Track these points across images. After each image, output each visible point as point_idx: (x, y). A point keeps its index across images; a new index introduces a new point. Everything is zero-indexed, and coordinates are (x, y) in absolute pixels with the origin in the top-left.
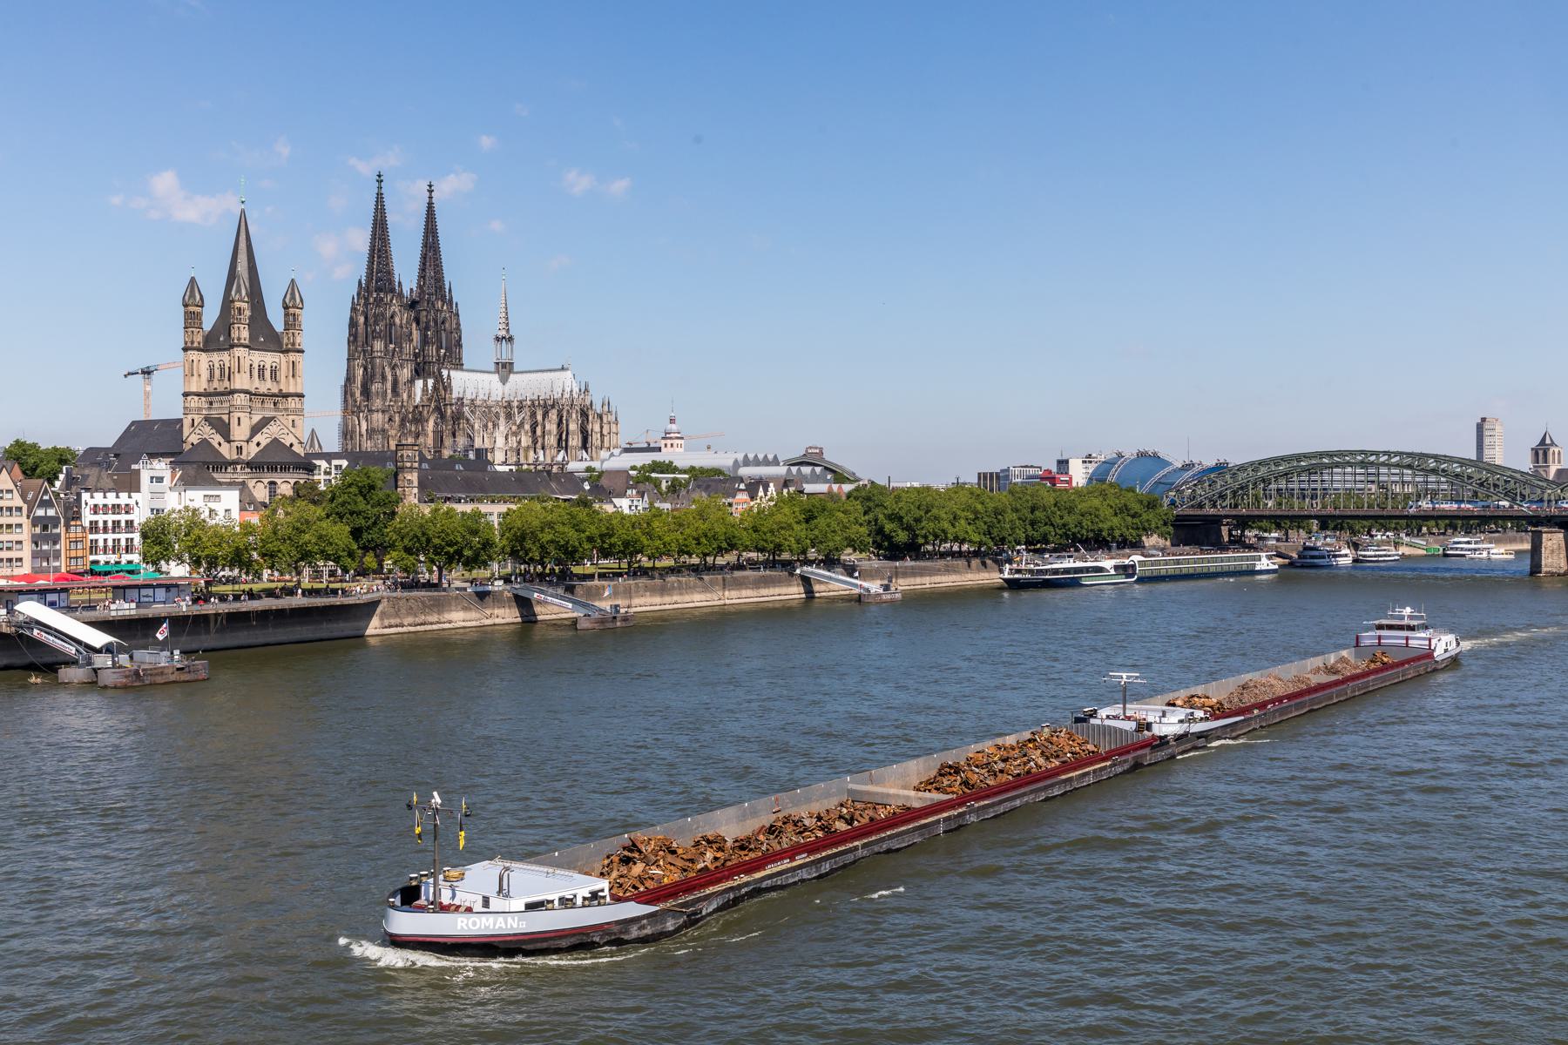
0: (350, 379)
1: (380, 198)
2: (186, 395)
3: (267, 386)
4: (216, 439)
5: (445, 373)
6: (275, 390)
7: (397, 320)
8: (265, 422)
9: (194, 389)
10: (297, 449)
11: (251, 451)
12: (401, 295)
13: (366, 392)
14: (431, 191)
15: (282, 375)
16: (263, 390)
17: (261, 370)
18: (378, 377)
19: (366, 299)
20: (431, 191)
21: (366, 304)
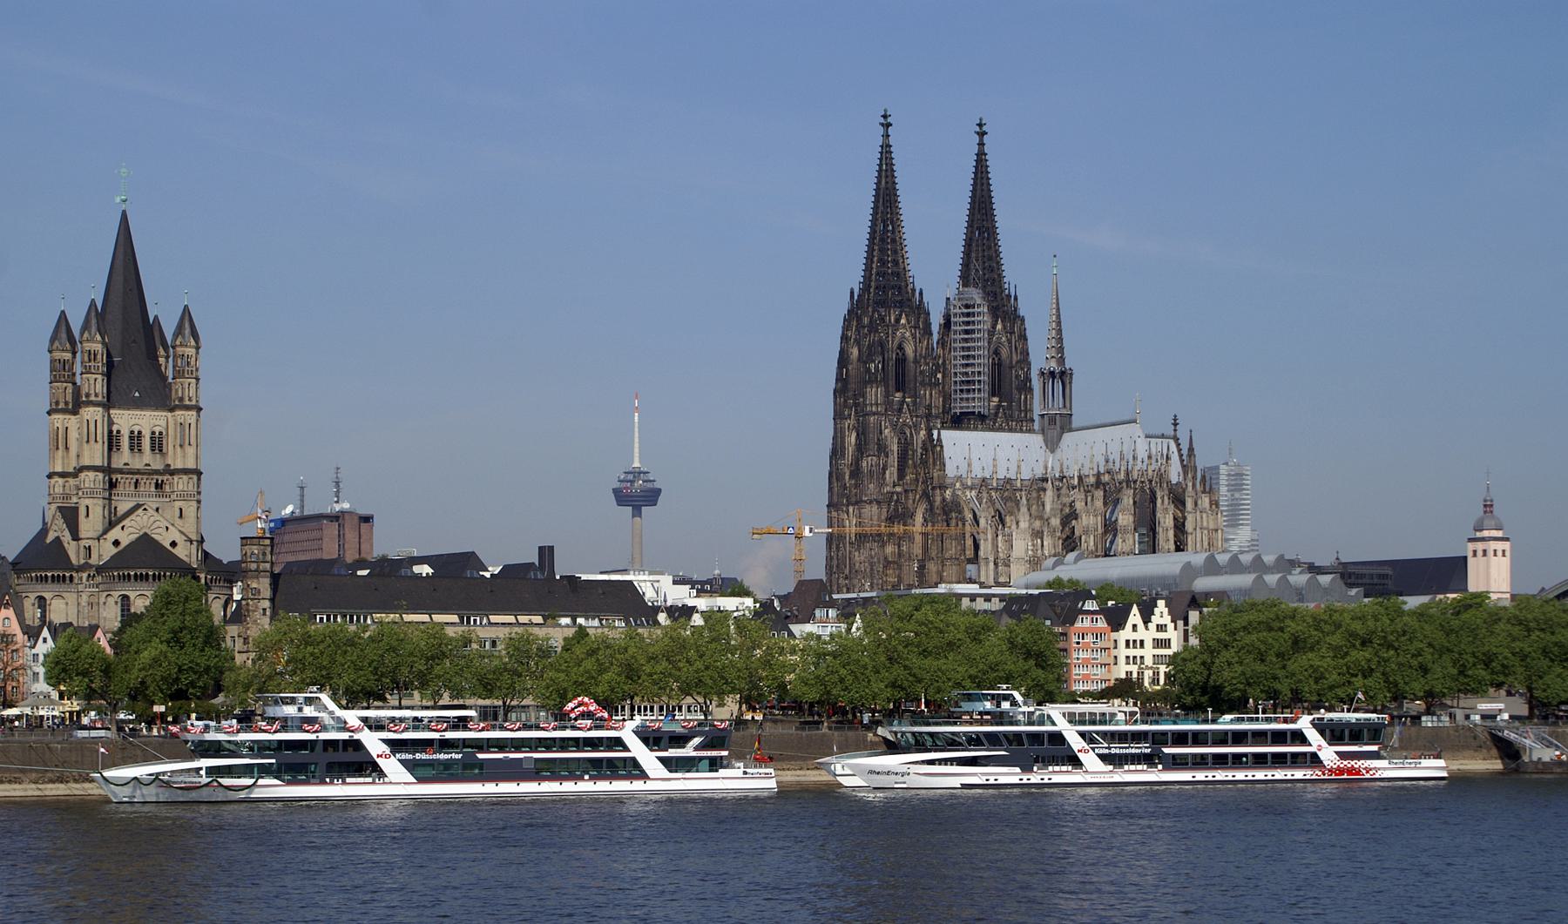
0: (837, 452)
1: (886, 151)
2: (50, 476)
3: (147, 458)
4: (66, 537)
5: (935, 433)
6: (158, 465)
7: (909, 350)
8: (138, 506)
9: (59, 469)
10: (181, 552)
11: (106, 551)
12: (919, 312)
13: (856, 472)
14: (982, 134)
15: (170, 445)
16: (137, 463)
17: (135, 439)
18: (873, 447)
19: (859, 319)
20: (982, 134)
21: (860, 326)
